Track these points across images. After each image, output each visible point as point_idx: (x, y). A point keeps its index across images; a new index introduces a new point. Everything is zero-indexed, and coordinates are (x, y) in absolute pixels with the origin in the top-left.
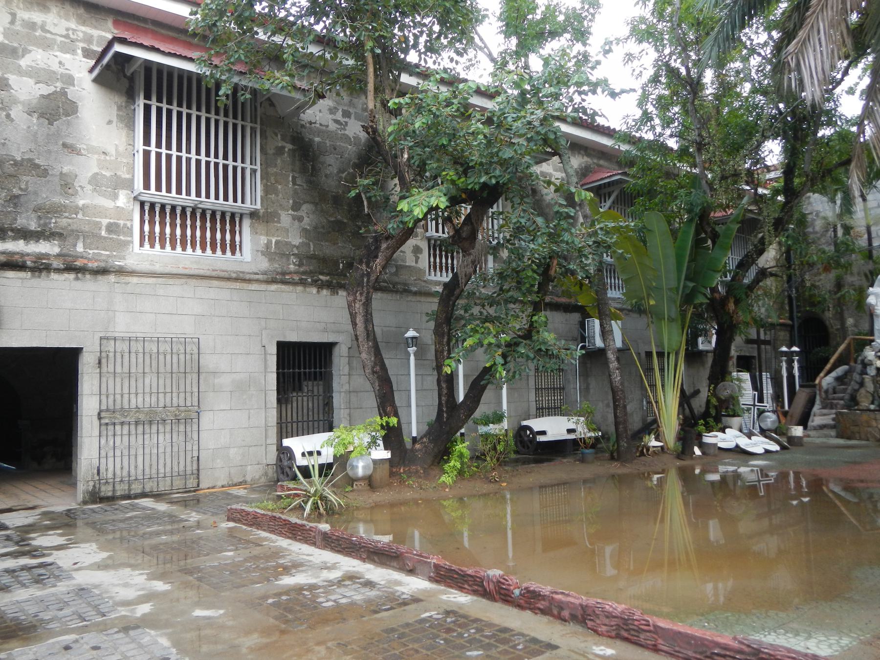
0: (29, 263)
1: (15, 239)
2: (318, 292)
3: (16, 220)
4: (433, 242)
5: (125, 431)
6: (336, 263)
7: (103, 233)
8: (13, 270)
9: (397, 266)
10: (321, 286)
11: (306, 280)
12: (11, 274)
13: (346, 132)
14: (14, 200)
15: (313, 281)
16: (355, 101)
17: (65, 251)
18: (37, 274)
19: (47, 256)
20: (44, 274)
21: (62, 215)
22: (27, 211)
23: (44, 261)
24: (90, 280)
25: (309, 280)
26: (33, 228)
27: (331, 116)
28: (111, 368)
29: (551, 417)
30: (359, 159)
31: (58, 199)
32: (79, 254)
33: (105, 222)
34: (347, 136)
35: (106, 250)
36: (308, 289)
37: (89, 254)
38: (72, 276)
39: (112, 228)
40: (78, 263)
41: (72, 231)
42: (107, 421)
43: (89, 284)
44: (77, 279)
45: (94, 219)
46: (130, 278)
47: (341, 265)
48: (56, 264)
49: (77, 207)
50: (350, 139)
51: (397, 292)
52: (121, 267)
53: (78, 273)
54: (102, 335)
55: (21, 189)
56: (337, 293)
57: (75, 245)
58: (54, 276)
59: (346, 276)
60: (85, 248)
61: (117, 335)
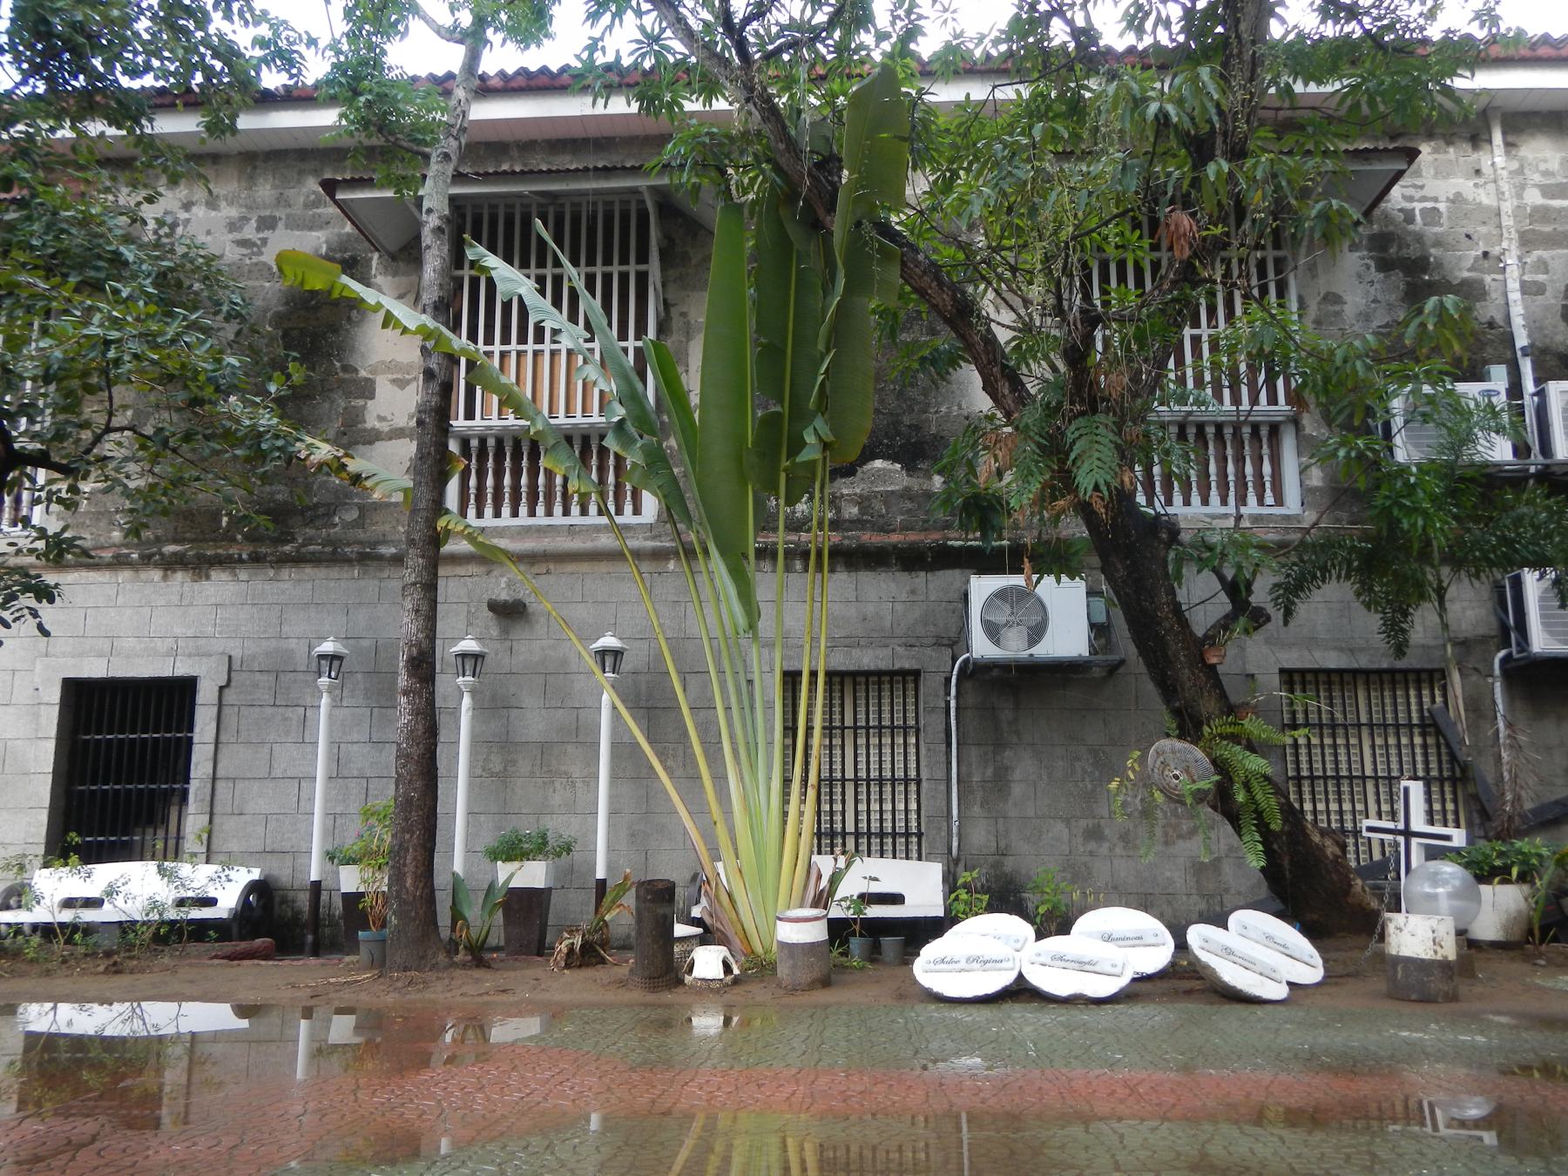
2: (165, 578)
4: (474, 443)
6: (216, 517)
9: (361, 508)
10: (171, 565)
11: (128, 555)
13: (262, 258)
15: (142, 557)
16: (291, 193)
25: (135, 556)
27: (230, 236)
29: (913, 863)
30: (287, 303)
34: (264, 264)
36: (143, 575)
47: (225, 519)
50: (270, 268)
51: (348, 561)
56: (208, 578)
59: (234, 540)
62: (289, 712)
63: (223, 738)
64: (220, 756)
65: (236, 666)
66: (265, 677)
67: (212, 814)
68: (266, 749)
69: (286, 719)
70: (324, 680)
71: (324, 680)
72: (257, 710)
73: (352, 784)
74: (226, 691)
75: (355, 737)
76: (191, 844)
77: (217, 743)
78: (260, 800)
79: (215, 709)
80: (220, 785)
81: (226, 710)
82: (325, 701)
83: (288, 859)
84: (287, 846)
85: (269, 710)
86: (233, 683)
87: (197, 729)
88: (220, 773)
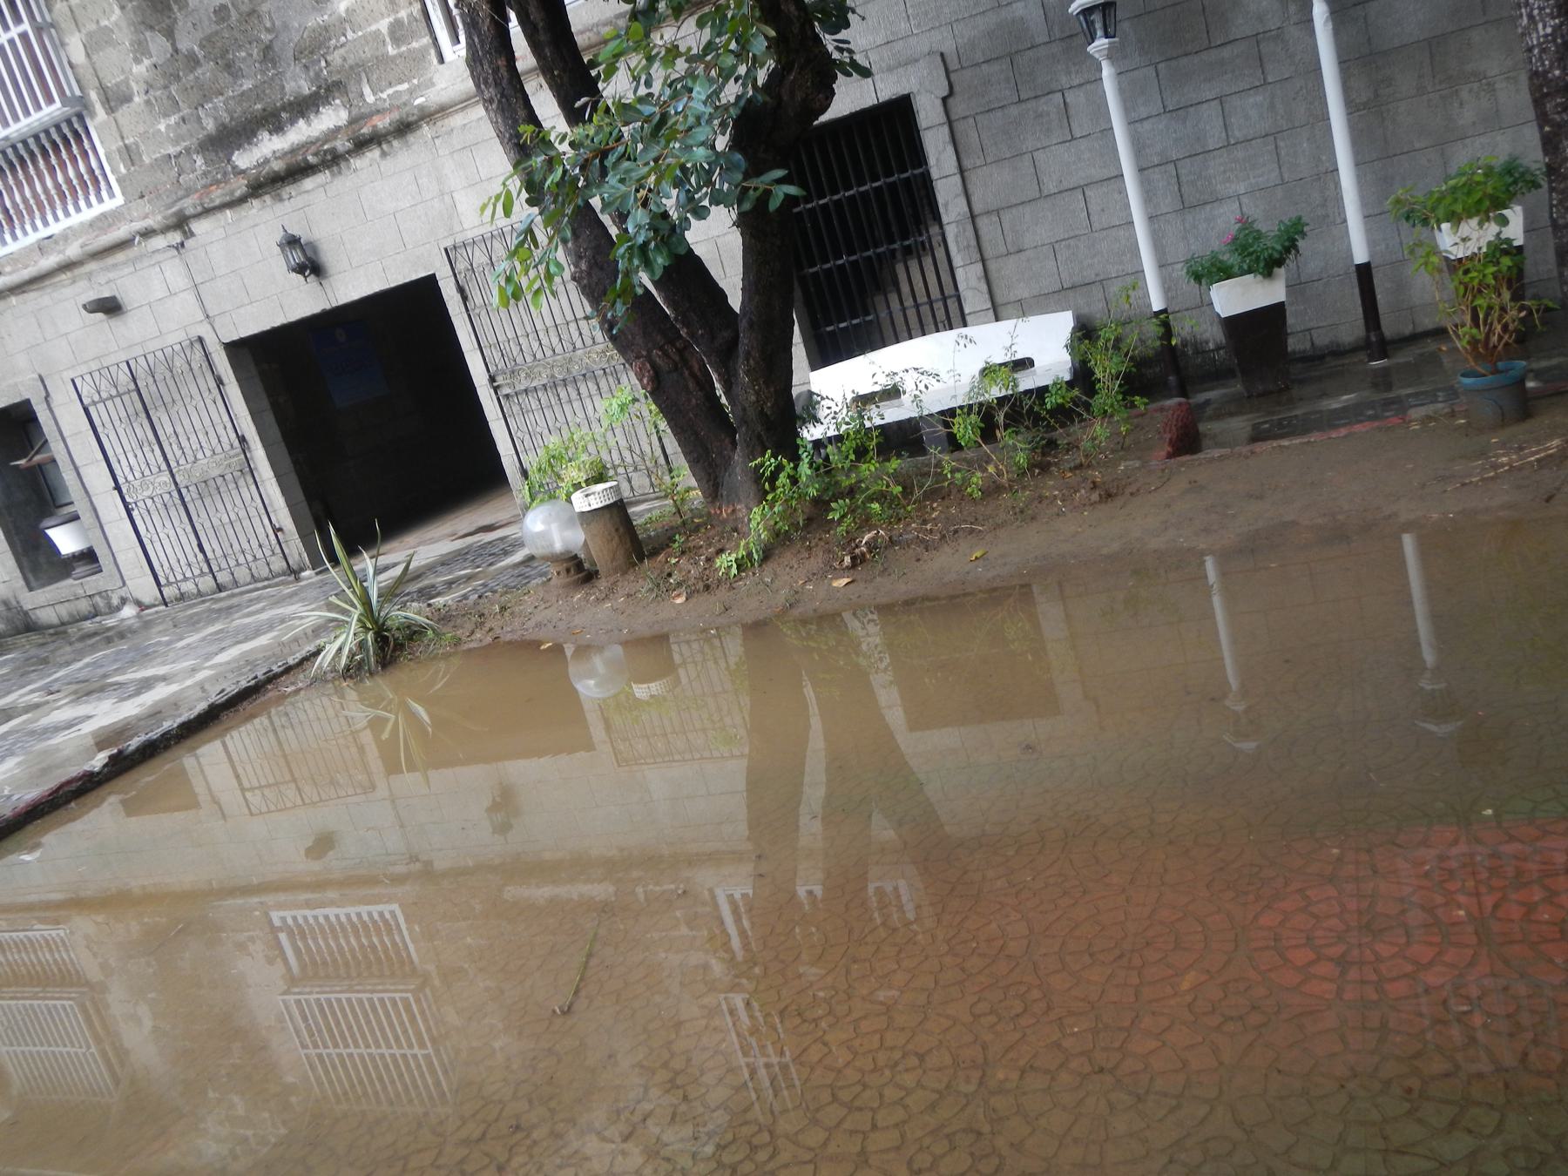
0: (310, 158)
1: (293, 122)
3: (283, 87)
5: (535, 404)
7: (391, 50)
8: (308, 176)
12: (309, 183)
14: (268, 54)
17: (355, 111)
18: (335, 168)
19: (334, 133)
20: (343, 165)
21: (329, 48)
22: (289, 65)
23: (326, 147)
24: (401, 149)
26: (306, 92)
28: (479, 301)
31: (315, 20)
32: (373, 109)
33: (383, 25)
35: (401, 82)
37: (385, 100)
38: (373, 154)
39: (398, 33)
40: (366, 130)
41: (351, 67)
42: (506, 390)
43: (406, 157)
44: (384, 154)
45: (368, 30)
46: (450, 118)
48: (342, 144)
49: (343, 21)
52: (421, 108)
53: (380, 144)
54: (449, 243)
55: (268, 30)
57: (362, 95)
58: (356, 162)
60: (374, 93)
61: (470, 235)
62: (1042, 105)
63: (967, 163)
64: (969, 186)
65: (953, 65)
66: (996, 67)
67: (983, 261)
68: (1027, 157)
69: (1039, 116)
70: (1100, 44)
71: (1100, 44)
72: (999, 114)
73: (1155, 175)
74: (951, 101)
75: (1143, 112)
76: (974, 298)
77: (962, 171)
78: (1039, 228)
79: (946, 129)
80: (982, 223)
81: (959, 127)
82: (1107, 72)
83: (1097, 292)
84: (1090, 275)
85: (1014, 111)
86: (957, 89)
87: (932, 161)
88: (977, 208)
